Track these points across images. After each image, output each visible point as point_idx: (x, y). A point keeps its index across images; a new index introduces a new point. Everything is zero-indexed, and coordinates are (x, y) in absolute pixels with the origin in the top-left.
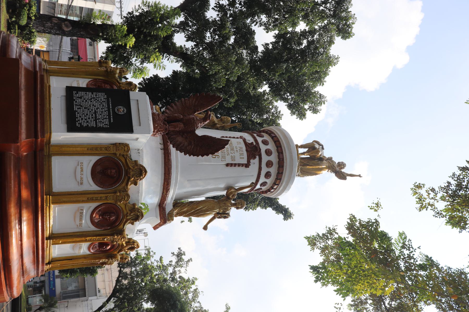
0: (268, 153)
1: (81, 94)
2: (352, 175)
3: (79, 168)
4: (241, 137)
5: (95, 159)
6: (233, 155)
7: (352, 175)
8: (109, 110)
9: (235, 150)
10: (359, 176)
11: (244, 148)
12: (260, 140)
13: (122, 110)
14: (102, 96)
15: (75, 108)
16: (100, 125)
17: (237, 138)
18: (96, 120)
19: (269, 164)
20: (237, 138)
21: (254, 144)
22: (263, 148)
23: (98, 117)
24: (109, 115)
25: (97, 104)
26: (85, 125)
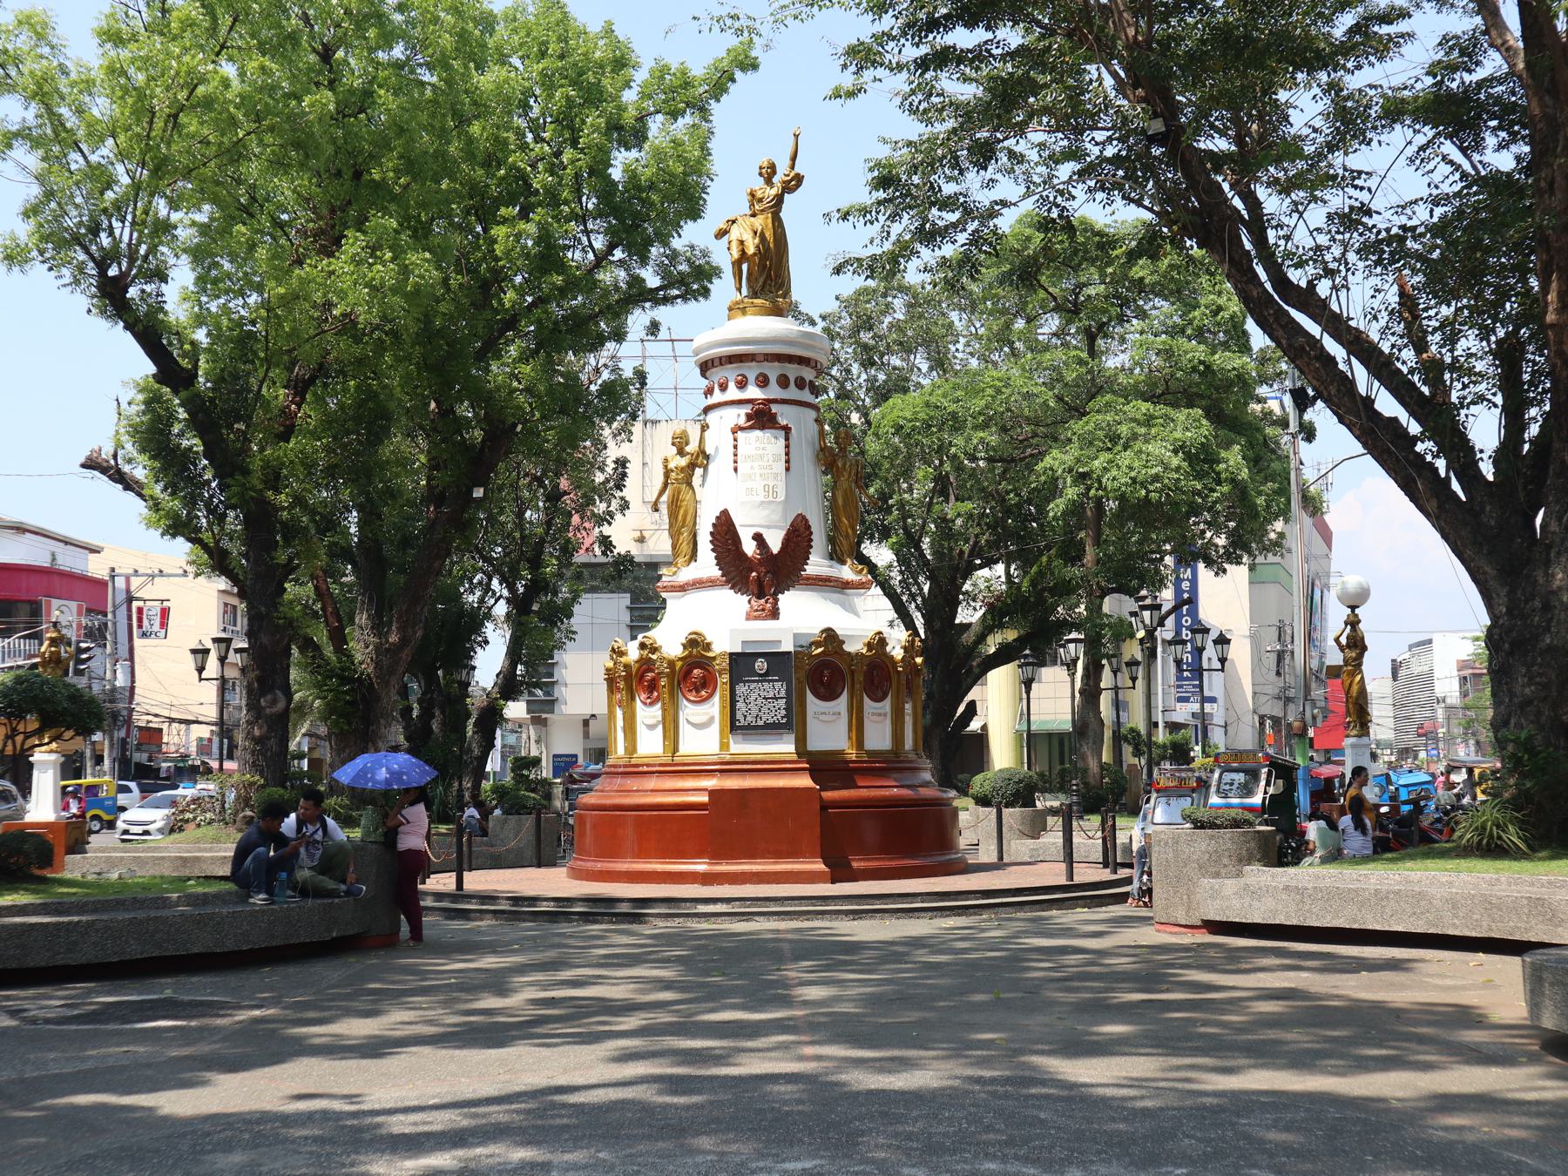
0: (763, 382)
1: (739, 716)
2: (794, 158)
3: (821, 717)
4: (734, 432)
5: (810, 697)
6: (771, 458)
7: (794, 158)
8: (762, 681)
9: (761, 452)
10: (796, 136)
11: (757, 433)
12: (733, 393)
13: (761, 665)
14: (741, 689)
15: (761, 723)
16: (783, 693)
17: (735, 440)
18: (777, 699)
19: (783, 382)
20: (735, 440)
21: (747, 409)
22: (753, 392)
23: (771, 695)
24: (769, 681)
25: (756, 695)
26: (783, 712)
